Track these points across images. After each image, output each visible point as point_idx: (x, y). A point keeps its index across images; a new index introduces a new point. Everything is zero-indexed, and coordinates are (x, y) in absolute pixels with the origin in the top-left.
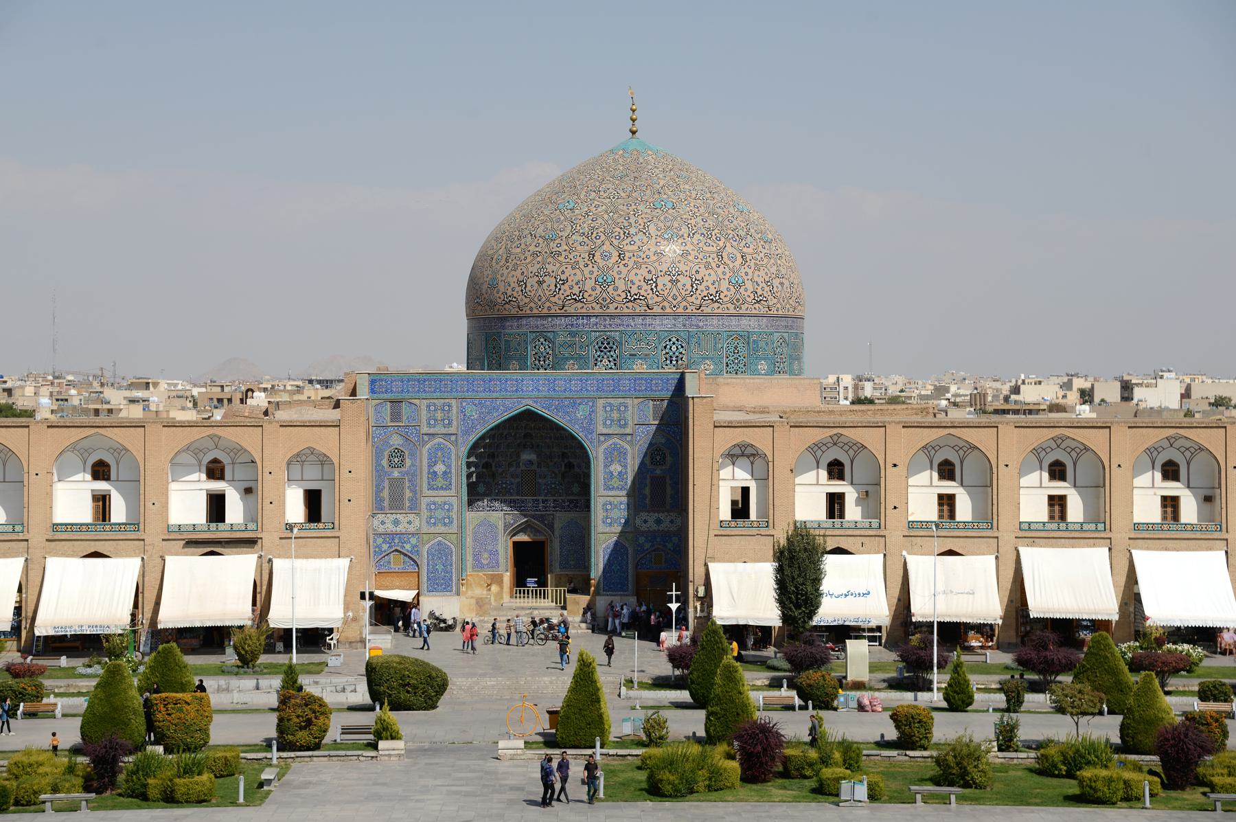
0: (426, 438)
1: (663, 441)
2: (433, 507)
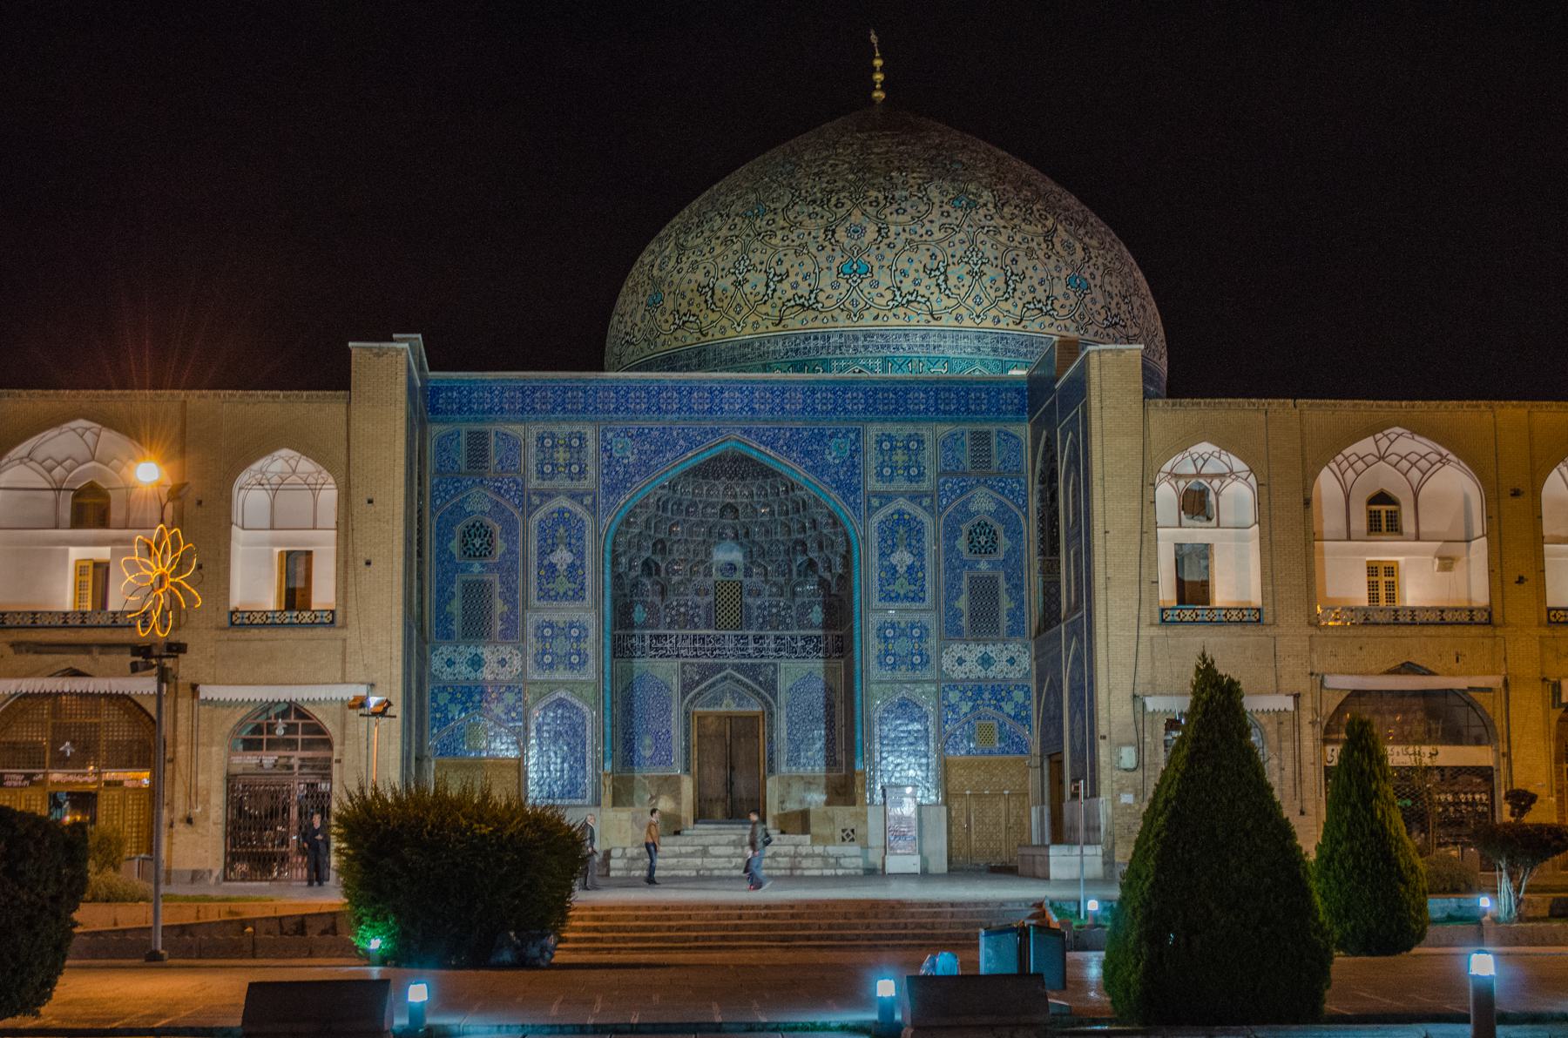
0: (536, 500)
1: (992, 507)
2: (548, 632)
